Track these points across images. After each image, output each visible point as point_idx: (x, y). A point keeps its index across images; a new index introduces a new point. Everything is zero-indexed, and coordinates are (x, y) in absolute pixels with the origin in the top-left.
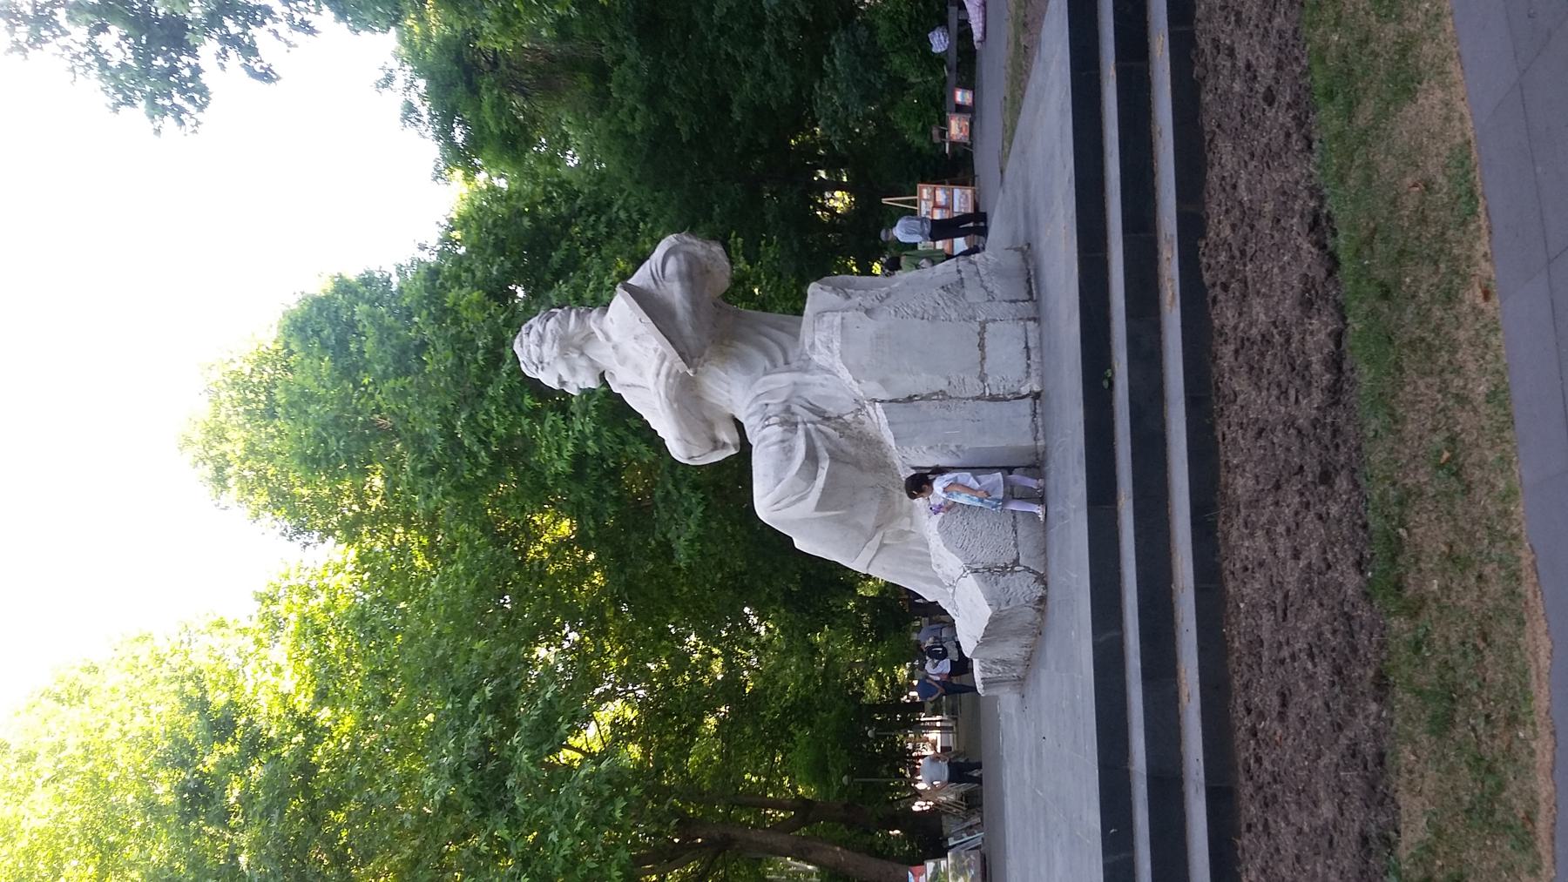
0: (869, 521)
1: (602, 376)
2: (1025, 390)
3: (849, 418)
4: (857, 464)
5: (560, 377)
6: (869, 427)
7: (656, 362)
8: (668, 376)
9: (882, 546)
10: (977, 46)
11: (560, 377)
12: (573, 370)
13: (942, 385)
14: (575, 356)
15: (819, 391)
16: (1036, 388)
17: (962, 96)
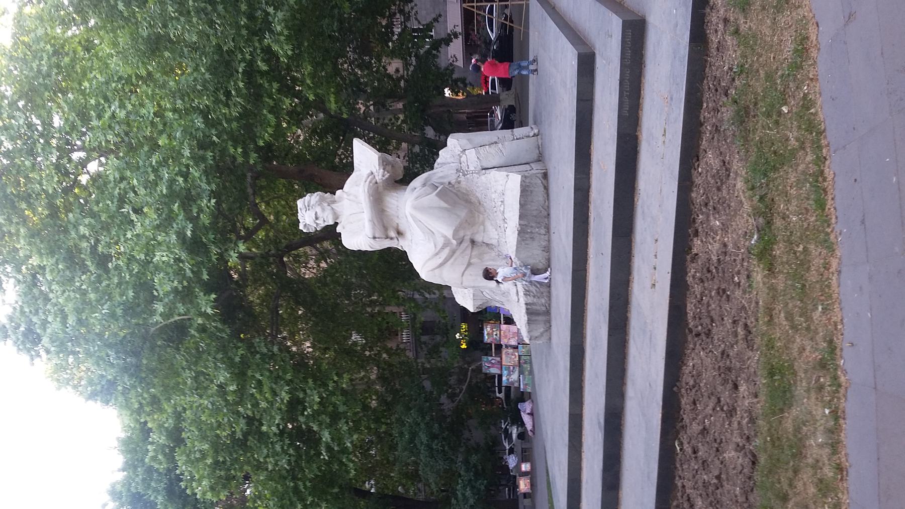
0: (463, 213)
1: (336, 224)
2: (531, 134)
3: (453, 182)
4: (457, 195)
5: (316, 213)
6: (464, 184)
7: (365, 176)
8: (370, 182)
9: (469, 264)
10: (530, 433)
11: (316, 213)
12: (323, 210)
13: (495, 139)
14: (326, 205)
15: (441, 174)
16: (536, 131)
17: (525, 467)
